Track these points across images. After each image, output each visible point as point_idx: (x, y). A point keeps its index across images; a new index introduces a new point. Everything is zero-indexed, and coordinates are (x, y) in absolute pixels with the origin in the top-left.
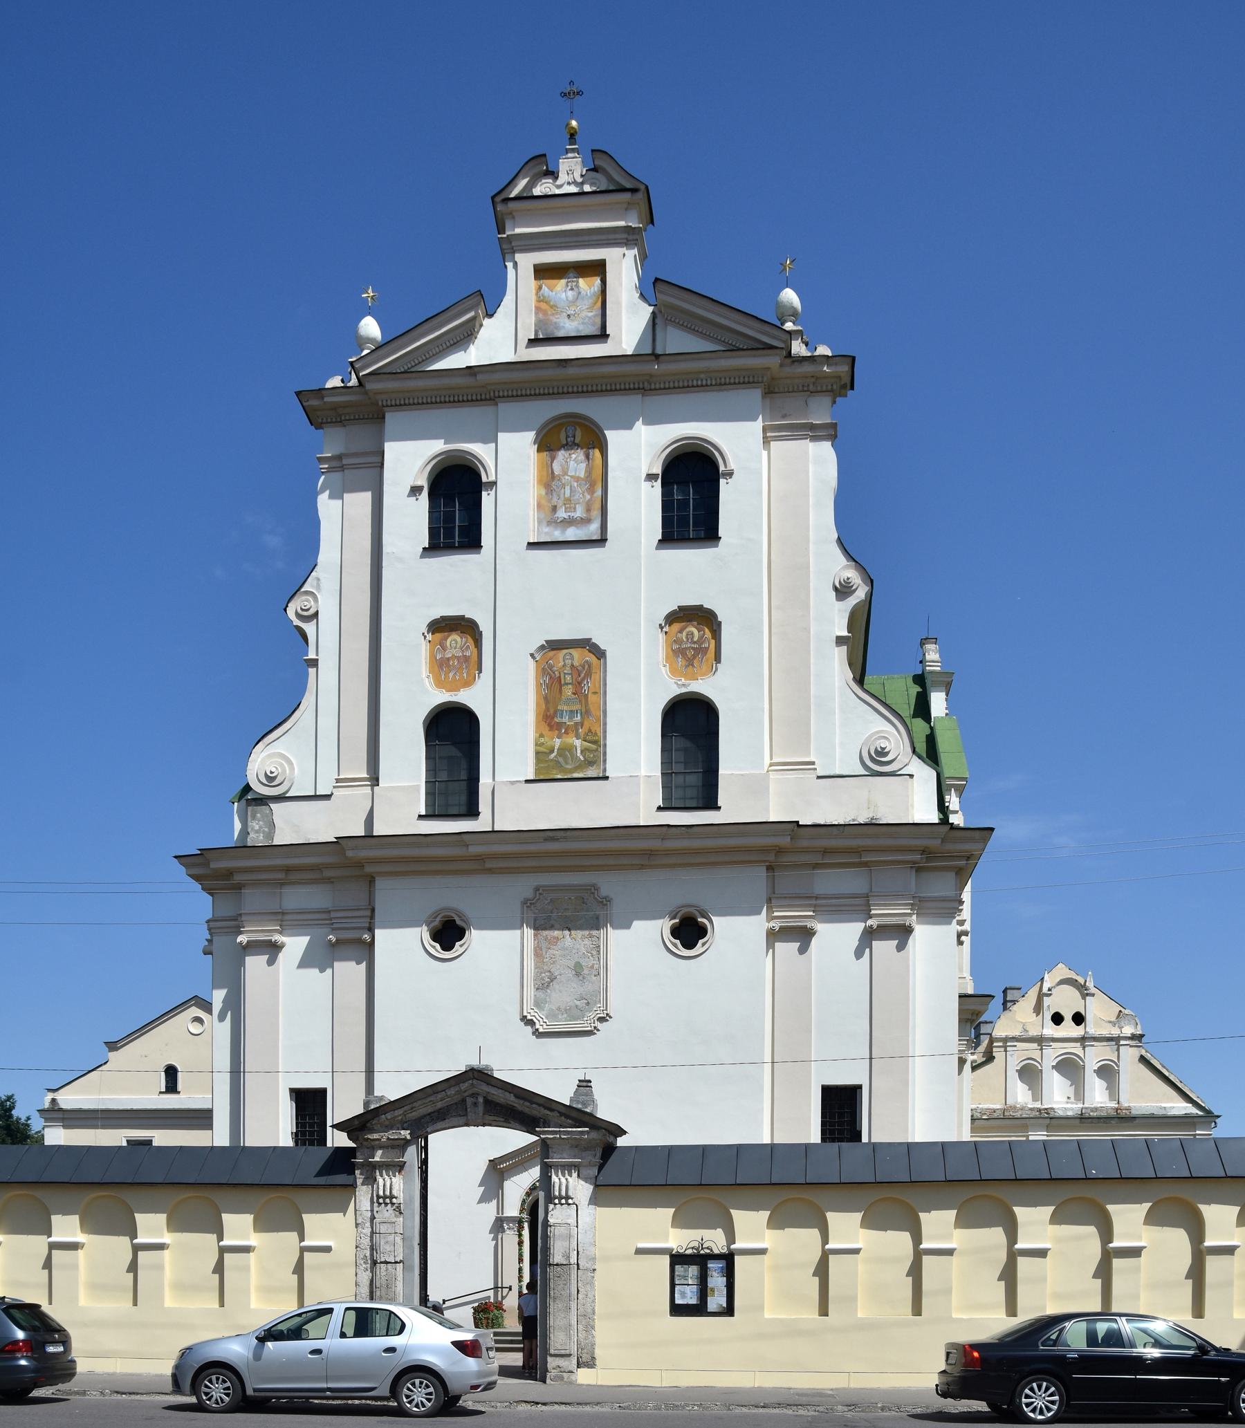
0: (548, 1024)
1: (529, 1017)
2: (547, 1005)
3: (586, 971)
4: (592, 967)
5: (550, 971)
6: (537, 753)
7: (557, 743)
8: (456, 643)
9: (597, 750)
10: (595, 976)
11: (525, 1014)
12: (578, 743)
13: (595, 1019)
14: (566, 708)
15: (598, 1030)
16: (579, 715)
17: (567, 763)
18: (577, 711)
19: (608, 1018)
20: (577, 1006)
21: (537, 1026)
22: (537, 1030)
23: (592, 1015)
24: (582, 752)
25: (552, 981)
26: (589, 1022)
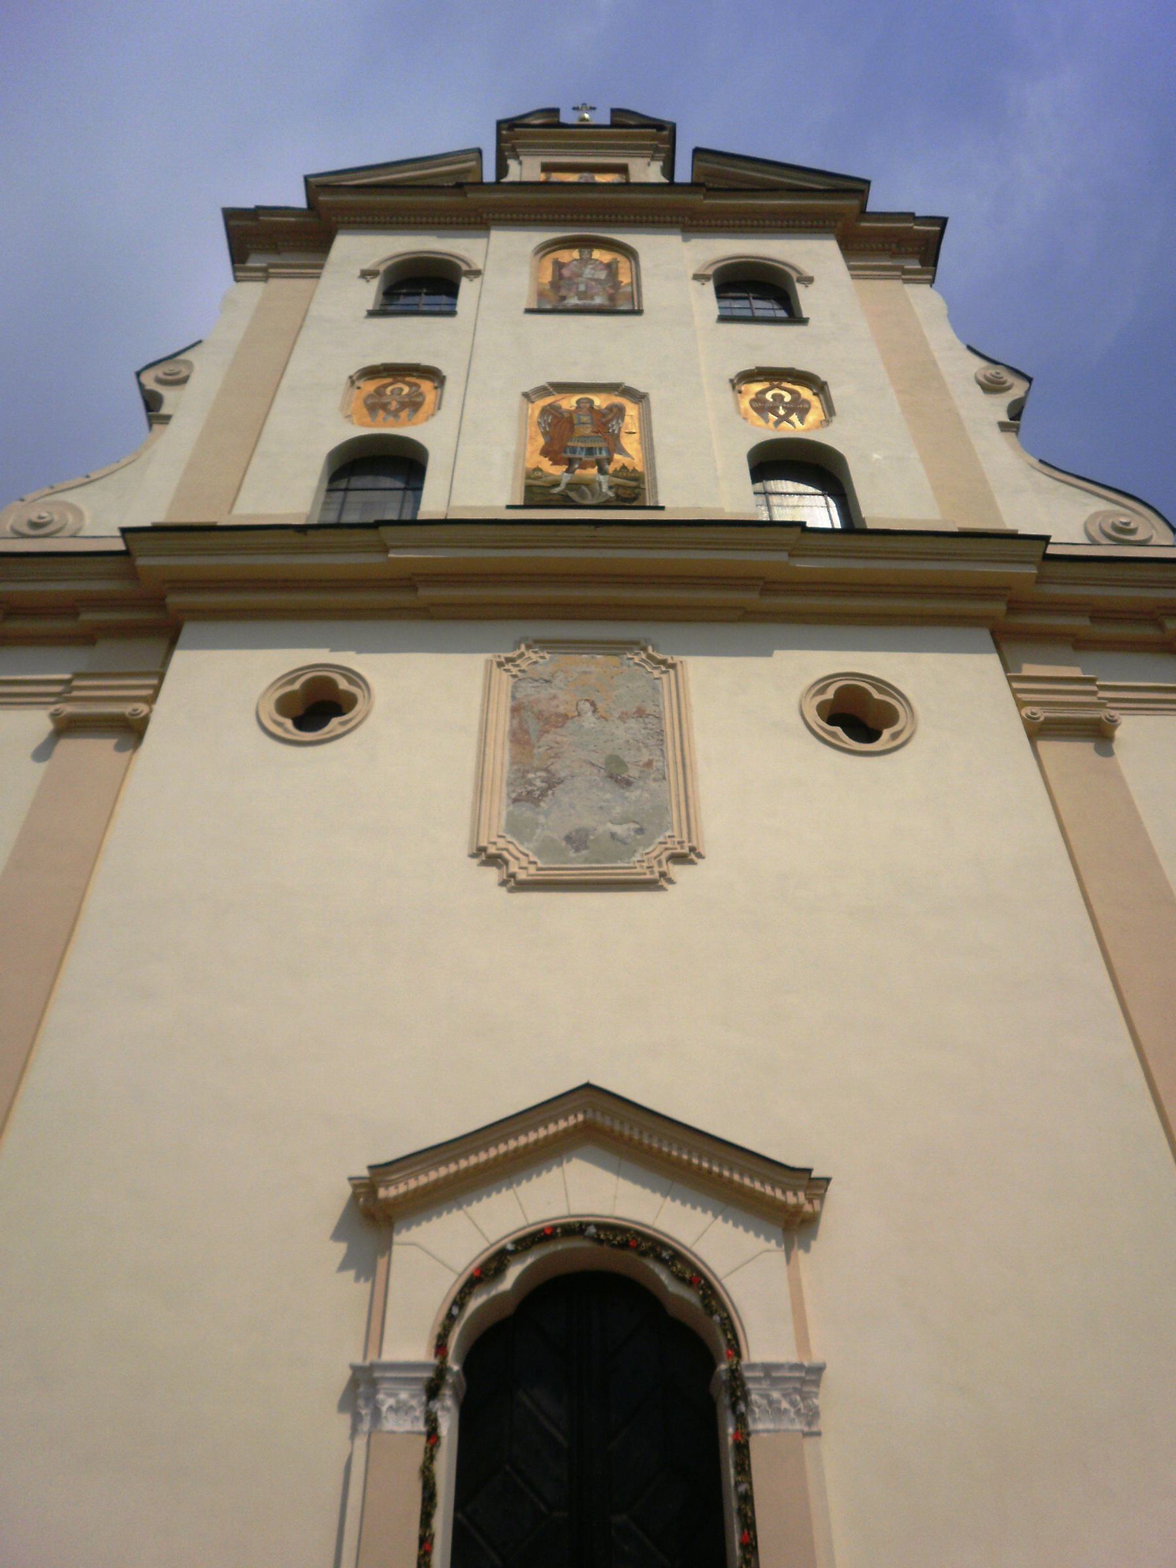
0: (540, 865)
1: (492, 850)
2: (538, 831)
3: (633, 772)
4: (649, 764)
5: (547, 770)
7: (566, 478)
8: (401, 390)
9: (638, 487)
10: (655, 780)
11: (484, 843)
12: (602, 478)
13: (663, 857)
14: (580, 444)
15: (671, 881)
18: (600, 449)
19: (693, 856)
20: (613, 836)
21: (514, 868)
22: (513, 876)
23: (655, 849)
24: (610, 488)
25: (550, 788)
26: (645, 864)
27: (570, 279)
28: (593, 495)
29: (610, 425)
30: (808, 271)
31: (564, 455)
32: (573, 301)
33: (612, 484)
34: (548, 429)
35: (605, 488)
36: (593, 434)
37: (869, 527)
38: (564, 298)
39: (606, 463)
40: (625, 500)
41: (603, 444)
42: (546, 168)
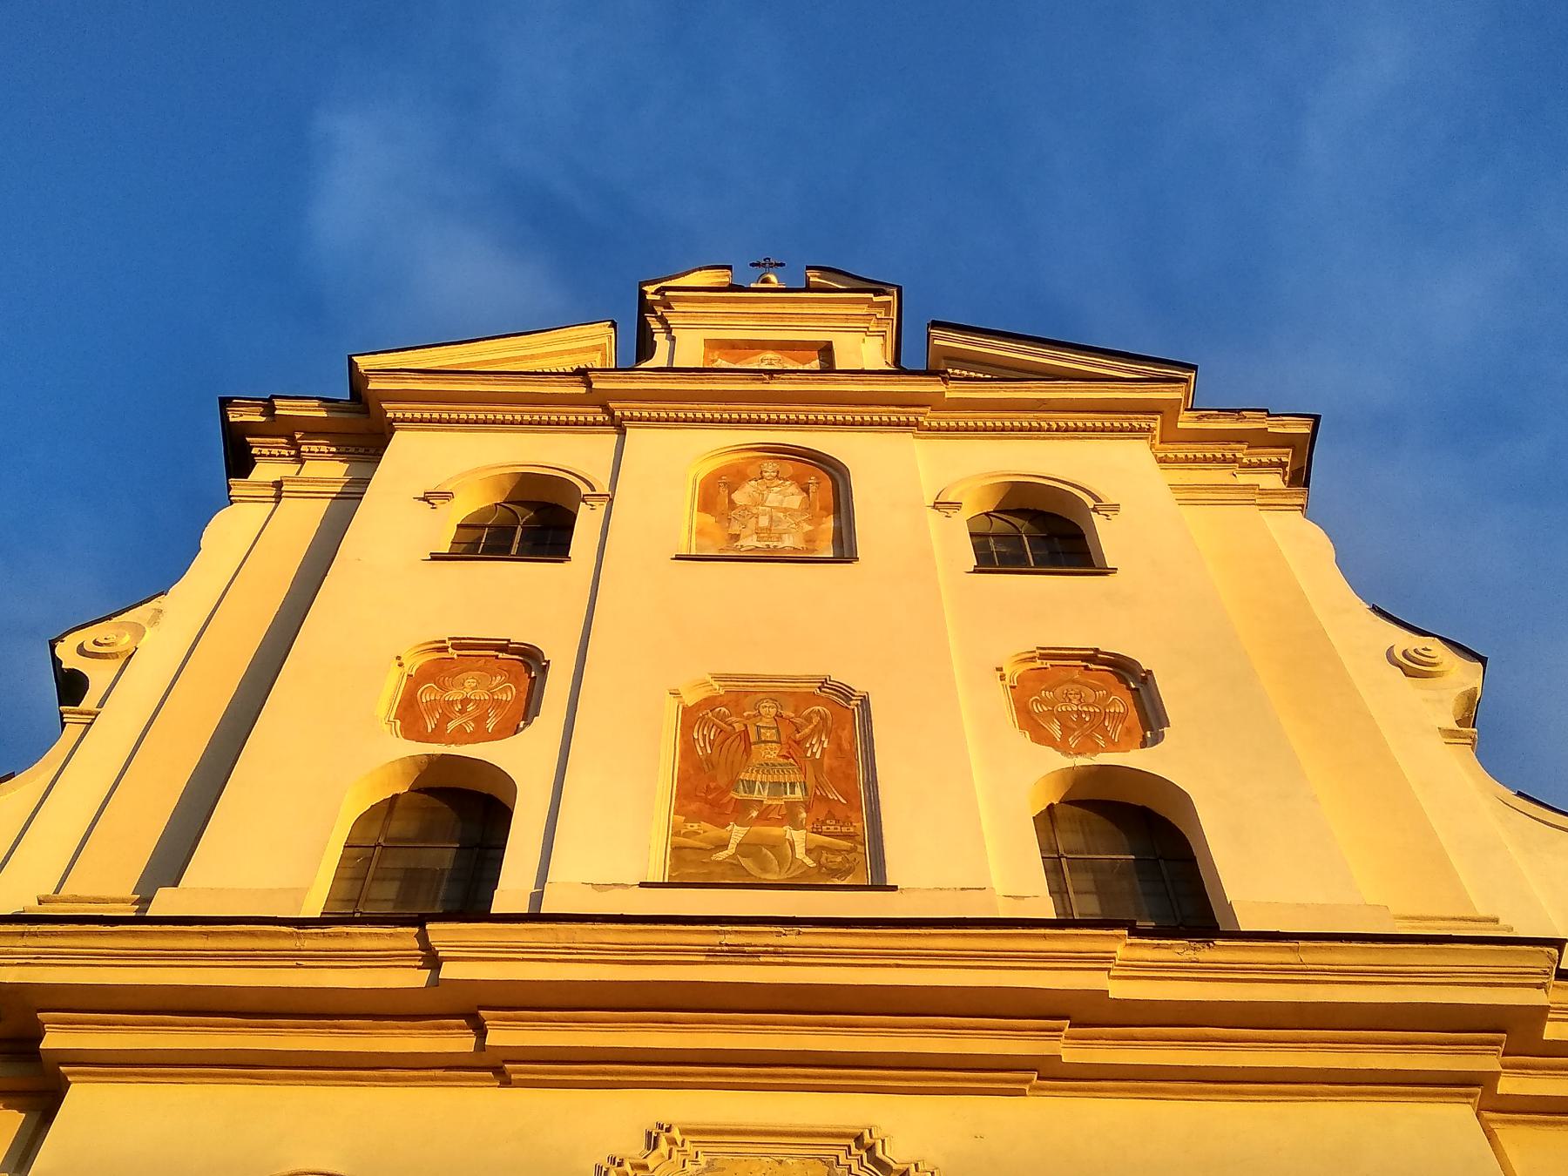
6: (677, 849)
9: (854, 850)
16: (798, 790)
17: (764, 870)
18: (793, 785)
24: (808, 852)
27: (746, 508)
28: (780, 865)
29: (808, 745)
30: (1109, 497)
31: (733, 795)
32: (749, 542)
33: (812, 847)
34: (709, 751)
35: (800, 852)
36: (781, 760)
37: (1242, 930)
38: (736, 537)
39: (802, 810)
40: (834, 873)
41: (799, 777)
42: (712, 345)
